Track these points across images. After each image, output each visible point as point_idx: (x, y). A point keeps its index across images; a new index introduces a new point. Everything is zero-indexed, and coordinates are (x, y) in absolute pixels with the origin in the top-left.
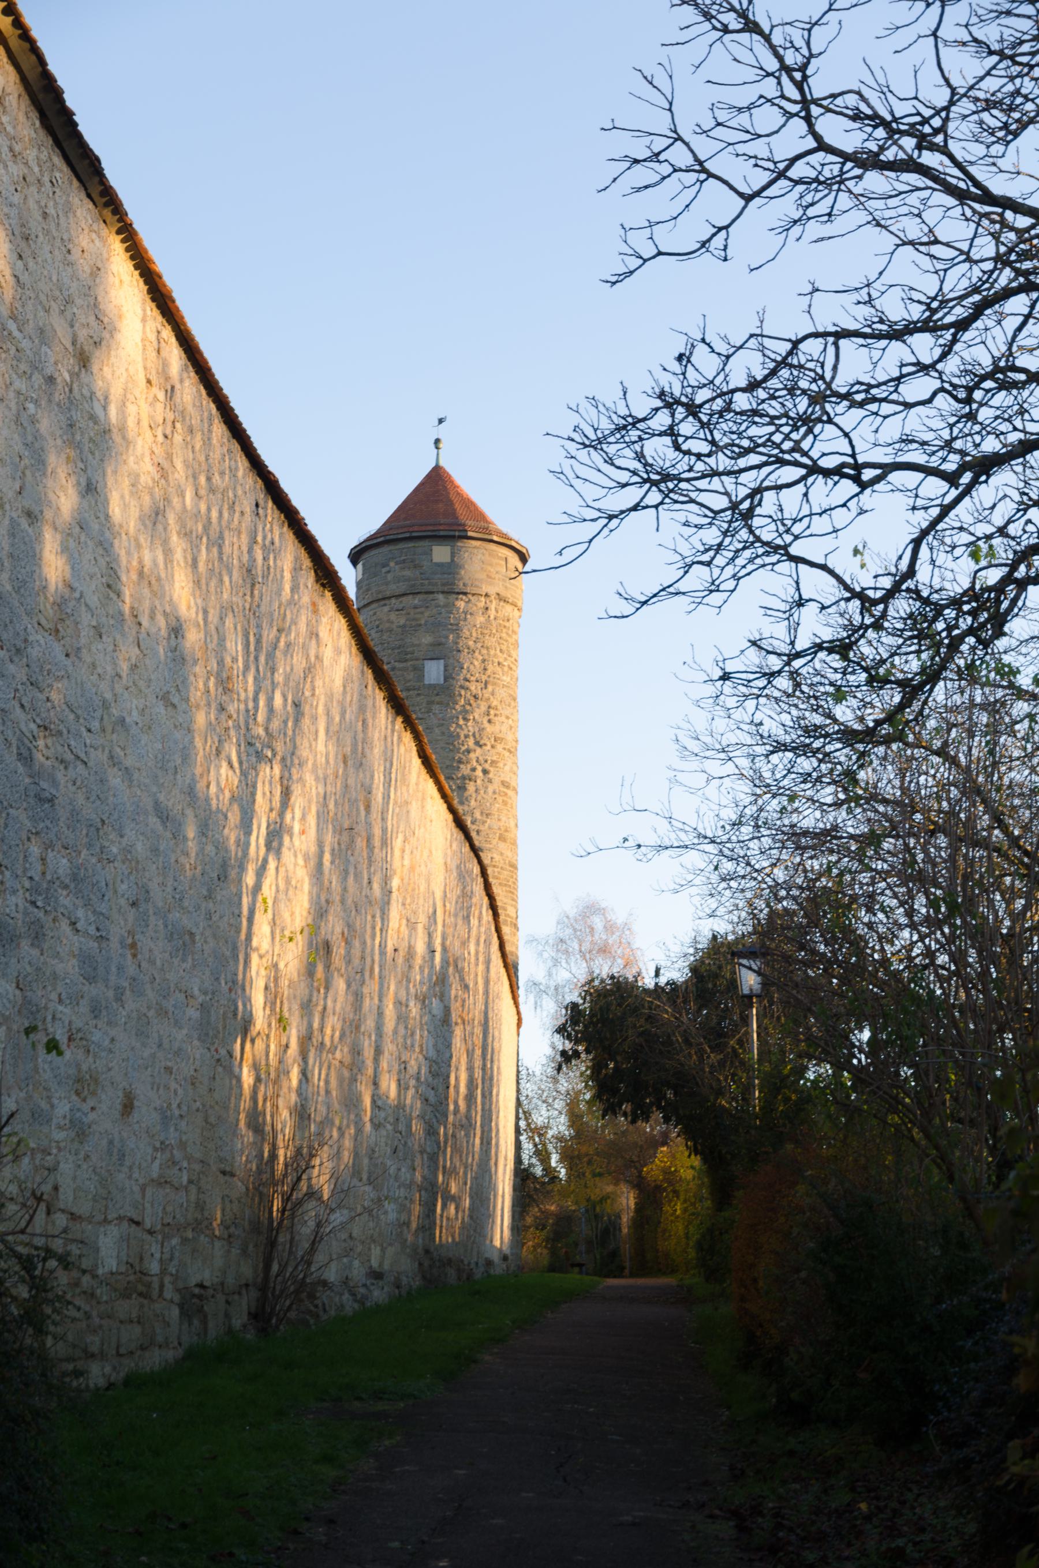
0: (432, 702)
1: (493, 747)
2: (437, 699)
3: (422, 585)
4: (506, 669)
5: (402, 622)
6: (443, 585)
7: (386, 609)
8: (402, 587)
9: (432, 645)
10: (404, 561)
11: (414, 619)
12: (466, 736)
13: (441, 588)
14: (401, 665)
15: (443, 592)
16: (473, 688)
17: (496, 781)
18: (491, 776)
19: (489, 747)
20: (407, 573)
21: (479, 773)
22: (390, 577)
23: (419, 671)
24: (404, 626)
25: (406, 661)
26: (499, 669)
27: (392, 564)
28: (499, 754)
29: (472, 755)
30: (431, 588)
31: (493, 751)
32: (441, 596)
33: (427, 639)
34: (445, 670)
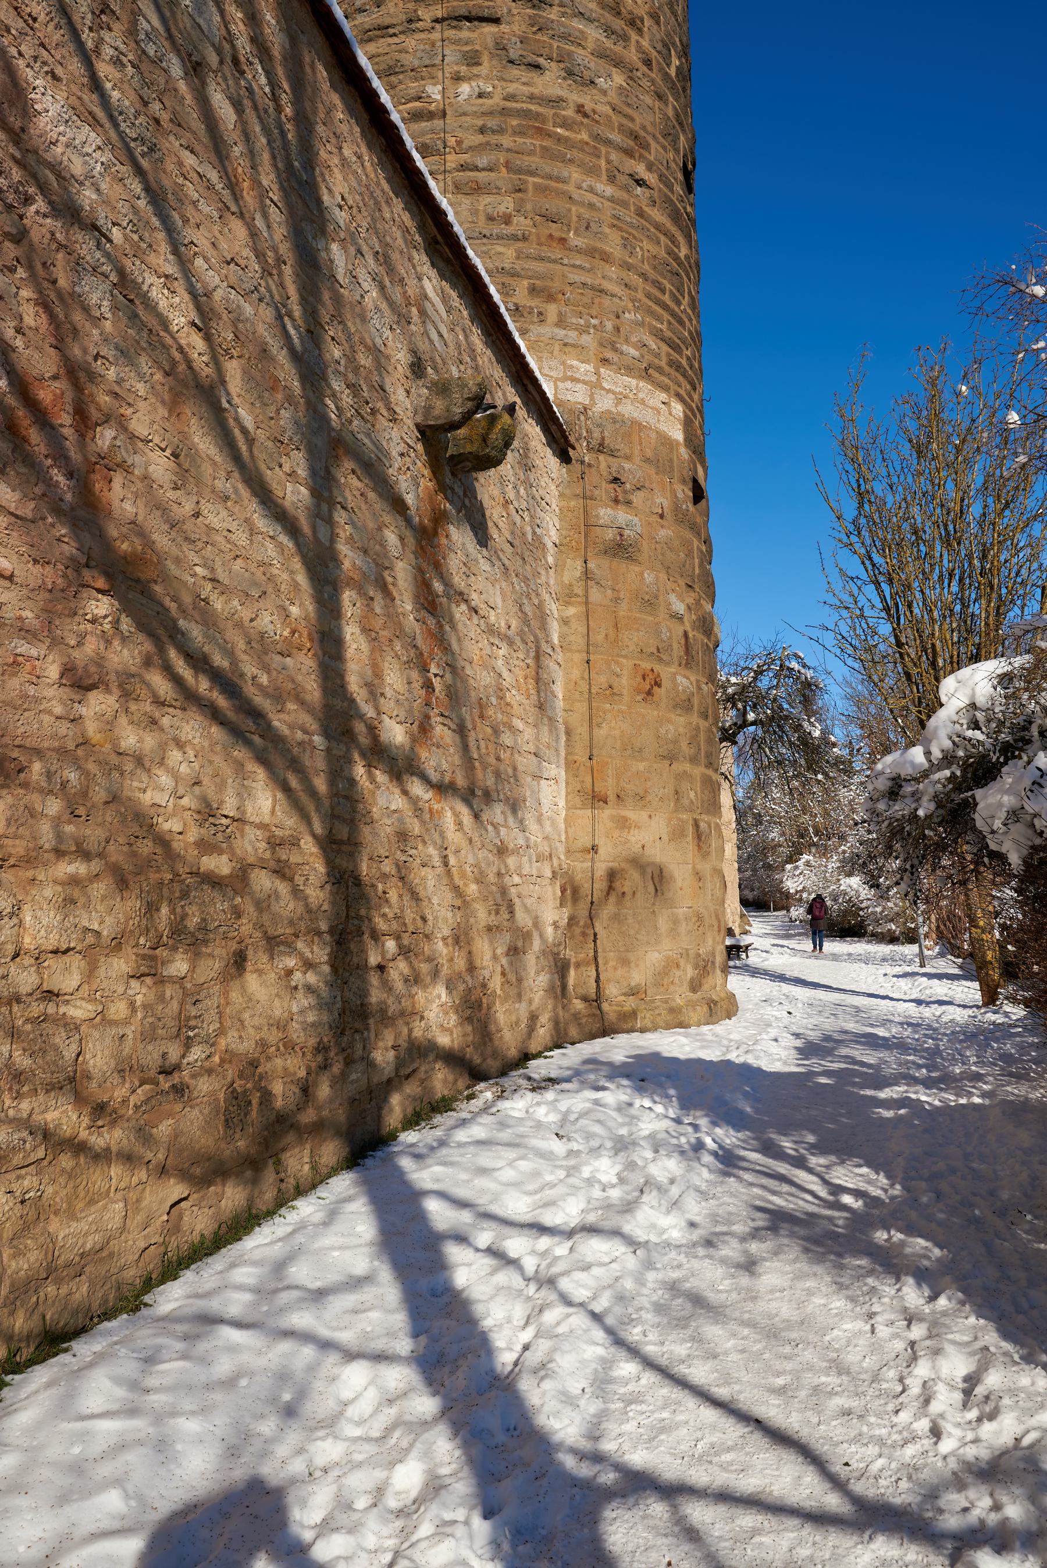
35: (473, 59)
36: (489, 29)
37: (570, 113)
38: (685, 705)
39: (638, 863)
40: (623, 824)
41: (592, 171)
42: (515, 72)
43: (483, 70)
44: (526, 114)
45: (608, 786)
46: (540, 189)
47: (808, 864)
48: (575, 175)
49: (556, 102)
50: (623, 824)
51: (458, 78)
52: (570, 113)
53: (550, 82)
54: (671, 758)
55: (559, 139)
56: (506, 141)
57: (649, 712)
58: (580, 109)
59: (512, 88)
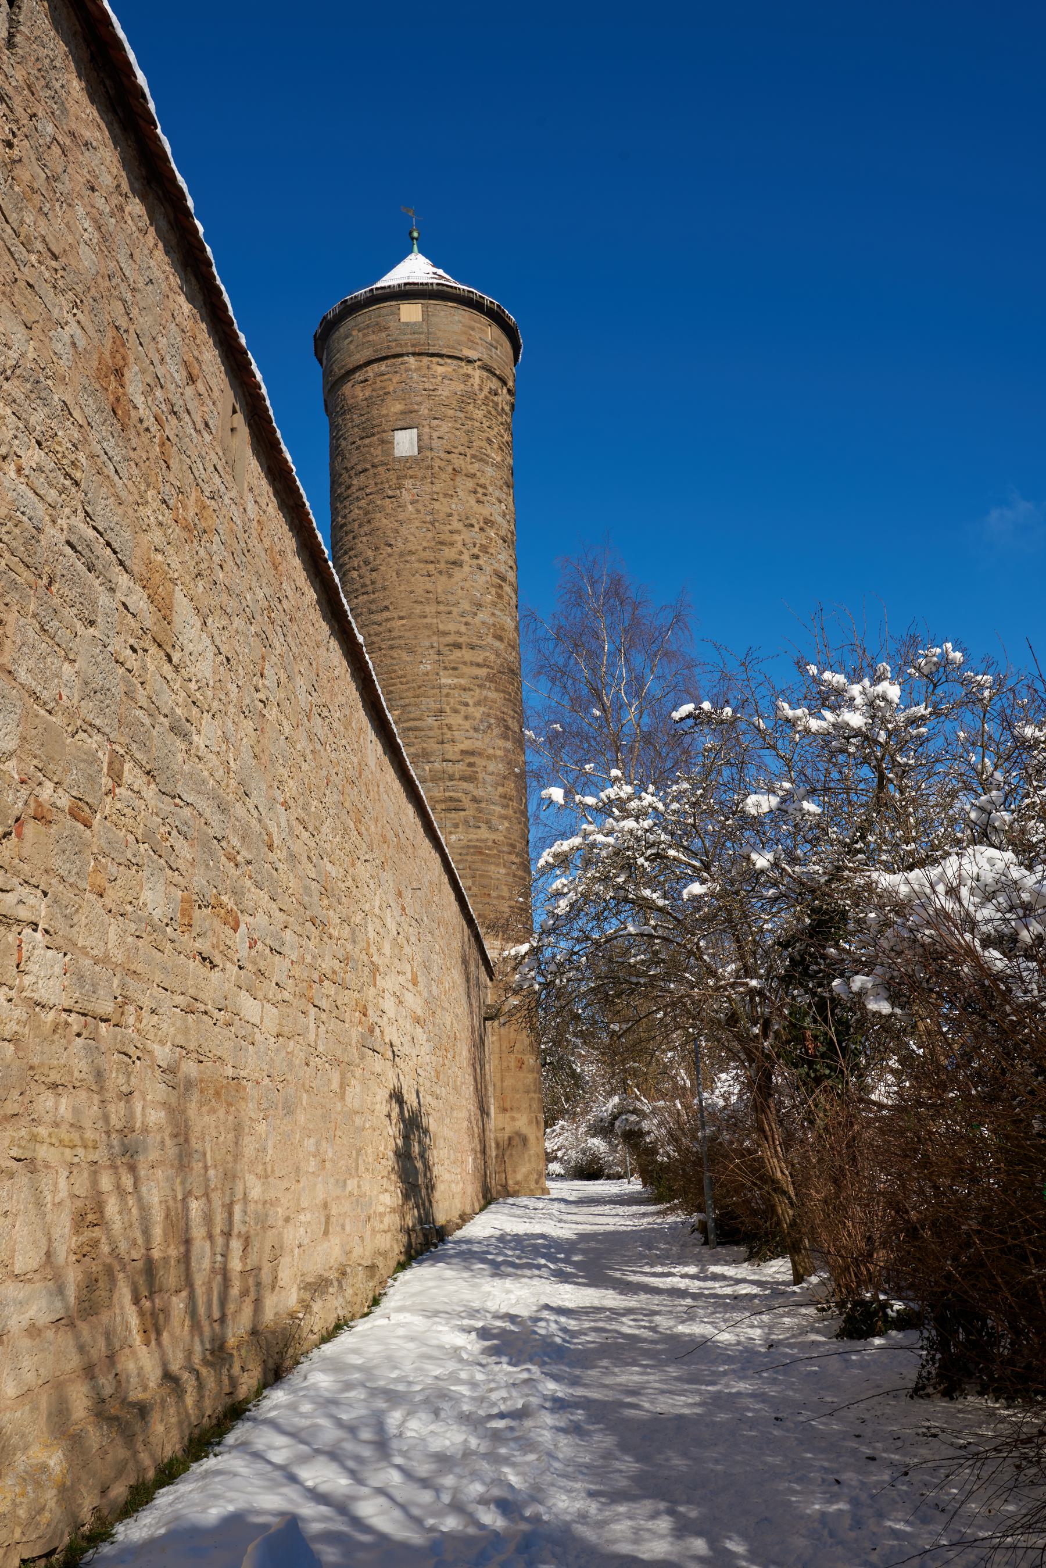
0: (405, 477)
1: (482, 529)
2: (411, 472)
3: (389, 347)
4: (496, 446)
5: (367, 393)
6: (413, 346)
7: (350, 384)
8: (367, 354)
9: (403, 413)
10: (368, 326)
11: (382, 388)
12: (450, 515)
13: (411, 350)
14: (367, 441)
15: (414, 354)
16: (455, 461)
17: (488, 569)
18: (481, 562)
19: (477, 527)
20: (372, 337)
21: (466, 557)
22: (352, 347)
23: (388, 444)
24: (371, 397)
25: (373, 435)
26: (484, 444)
27: (355, 333)
28: (487, 537)
29: (456, 537)
30: (398, 350)
31: (483, 534)
32: (411, 360)
33: (398, 407)
34: (419, 440)
35: (456, 826)
36: (462, 813)
37: (490, 844)
38: (532, 1071)
39: (518, 1134)
40: (513, 1119)
41: (498, 865)
42: (471, 830)
43: (460, 830)
44: (475, 847)
45: (508, 1105)
46: (481, 876)
47: (562, 1128)
48: (492, 867)
49: (485, 841)
50: (513, 1119)
51: (451, 833)
52: (490, 844)
53: (484, 833)
54: (528, 1092)
55: (488, 855)
56: (469, 858)
57: (521, 1075)
58: (494, 842)
59: (471, 836)
